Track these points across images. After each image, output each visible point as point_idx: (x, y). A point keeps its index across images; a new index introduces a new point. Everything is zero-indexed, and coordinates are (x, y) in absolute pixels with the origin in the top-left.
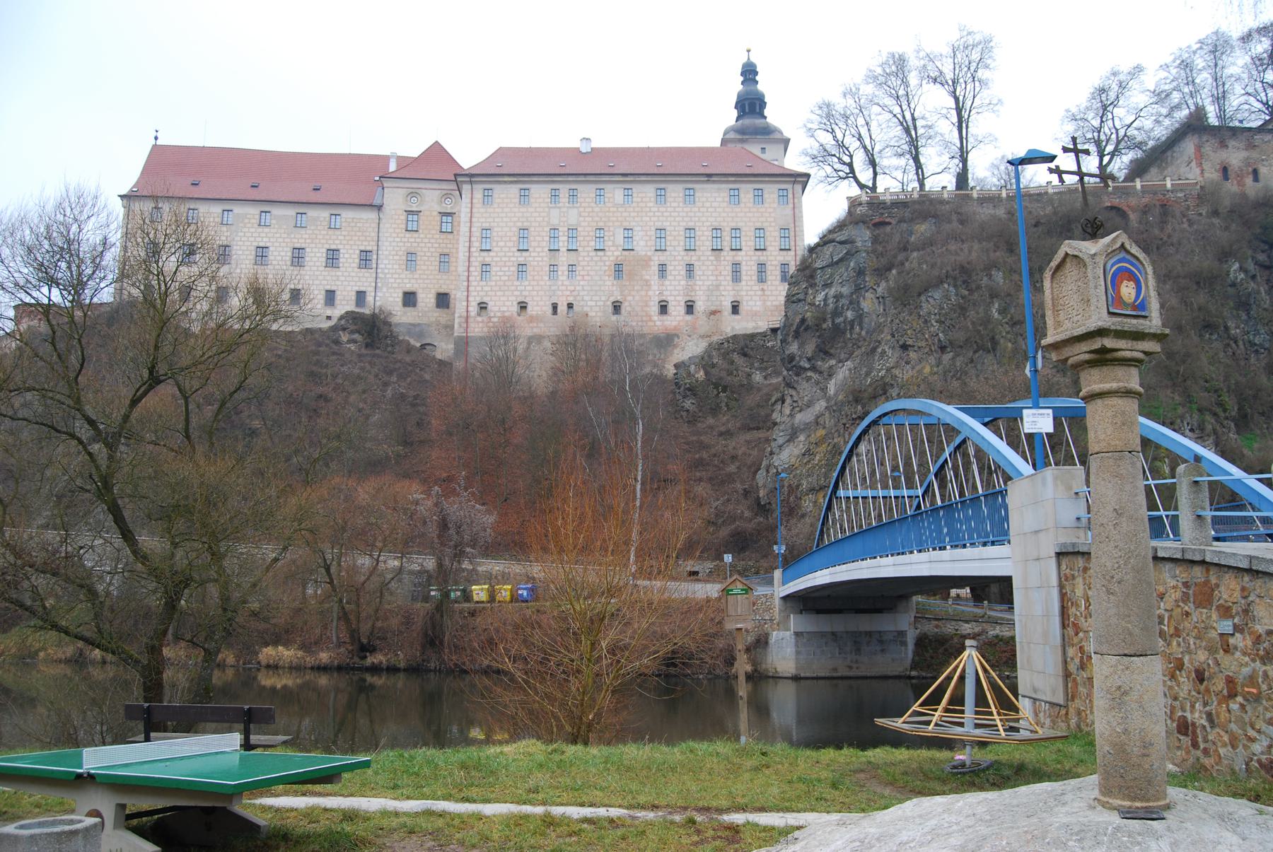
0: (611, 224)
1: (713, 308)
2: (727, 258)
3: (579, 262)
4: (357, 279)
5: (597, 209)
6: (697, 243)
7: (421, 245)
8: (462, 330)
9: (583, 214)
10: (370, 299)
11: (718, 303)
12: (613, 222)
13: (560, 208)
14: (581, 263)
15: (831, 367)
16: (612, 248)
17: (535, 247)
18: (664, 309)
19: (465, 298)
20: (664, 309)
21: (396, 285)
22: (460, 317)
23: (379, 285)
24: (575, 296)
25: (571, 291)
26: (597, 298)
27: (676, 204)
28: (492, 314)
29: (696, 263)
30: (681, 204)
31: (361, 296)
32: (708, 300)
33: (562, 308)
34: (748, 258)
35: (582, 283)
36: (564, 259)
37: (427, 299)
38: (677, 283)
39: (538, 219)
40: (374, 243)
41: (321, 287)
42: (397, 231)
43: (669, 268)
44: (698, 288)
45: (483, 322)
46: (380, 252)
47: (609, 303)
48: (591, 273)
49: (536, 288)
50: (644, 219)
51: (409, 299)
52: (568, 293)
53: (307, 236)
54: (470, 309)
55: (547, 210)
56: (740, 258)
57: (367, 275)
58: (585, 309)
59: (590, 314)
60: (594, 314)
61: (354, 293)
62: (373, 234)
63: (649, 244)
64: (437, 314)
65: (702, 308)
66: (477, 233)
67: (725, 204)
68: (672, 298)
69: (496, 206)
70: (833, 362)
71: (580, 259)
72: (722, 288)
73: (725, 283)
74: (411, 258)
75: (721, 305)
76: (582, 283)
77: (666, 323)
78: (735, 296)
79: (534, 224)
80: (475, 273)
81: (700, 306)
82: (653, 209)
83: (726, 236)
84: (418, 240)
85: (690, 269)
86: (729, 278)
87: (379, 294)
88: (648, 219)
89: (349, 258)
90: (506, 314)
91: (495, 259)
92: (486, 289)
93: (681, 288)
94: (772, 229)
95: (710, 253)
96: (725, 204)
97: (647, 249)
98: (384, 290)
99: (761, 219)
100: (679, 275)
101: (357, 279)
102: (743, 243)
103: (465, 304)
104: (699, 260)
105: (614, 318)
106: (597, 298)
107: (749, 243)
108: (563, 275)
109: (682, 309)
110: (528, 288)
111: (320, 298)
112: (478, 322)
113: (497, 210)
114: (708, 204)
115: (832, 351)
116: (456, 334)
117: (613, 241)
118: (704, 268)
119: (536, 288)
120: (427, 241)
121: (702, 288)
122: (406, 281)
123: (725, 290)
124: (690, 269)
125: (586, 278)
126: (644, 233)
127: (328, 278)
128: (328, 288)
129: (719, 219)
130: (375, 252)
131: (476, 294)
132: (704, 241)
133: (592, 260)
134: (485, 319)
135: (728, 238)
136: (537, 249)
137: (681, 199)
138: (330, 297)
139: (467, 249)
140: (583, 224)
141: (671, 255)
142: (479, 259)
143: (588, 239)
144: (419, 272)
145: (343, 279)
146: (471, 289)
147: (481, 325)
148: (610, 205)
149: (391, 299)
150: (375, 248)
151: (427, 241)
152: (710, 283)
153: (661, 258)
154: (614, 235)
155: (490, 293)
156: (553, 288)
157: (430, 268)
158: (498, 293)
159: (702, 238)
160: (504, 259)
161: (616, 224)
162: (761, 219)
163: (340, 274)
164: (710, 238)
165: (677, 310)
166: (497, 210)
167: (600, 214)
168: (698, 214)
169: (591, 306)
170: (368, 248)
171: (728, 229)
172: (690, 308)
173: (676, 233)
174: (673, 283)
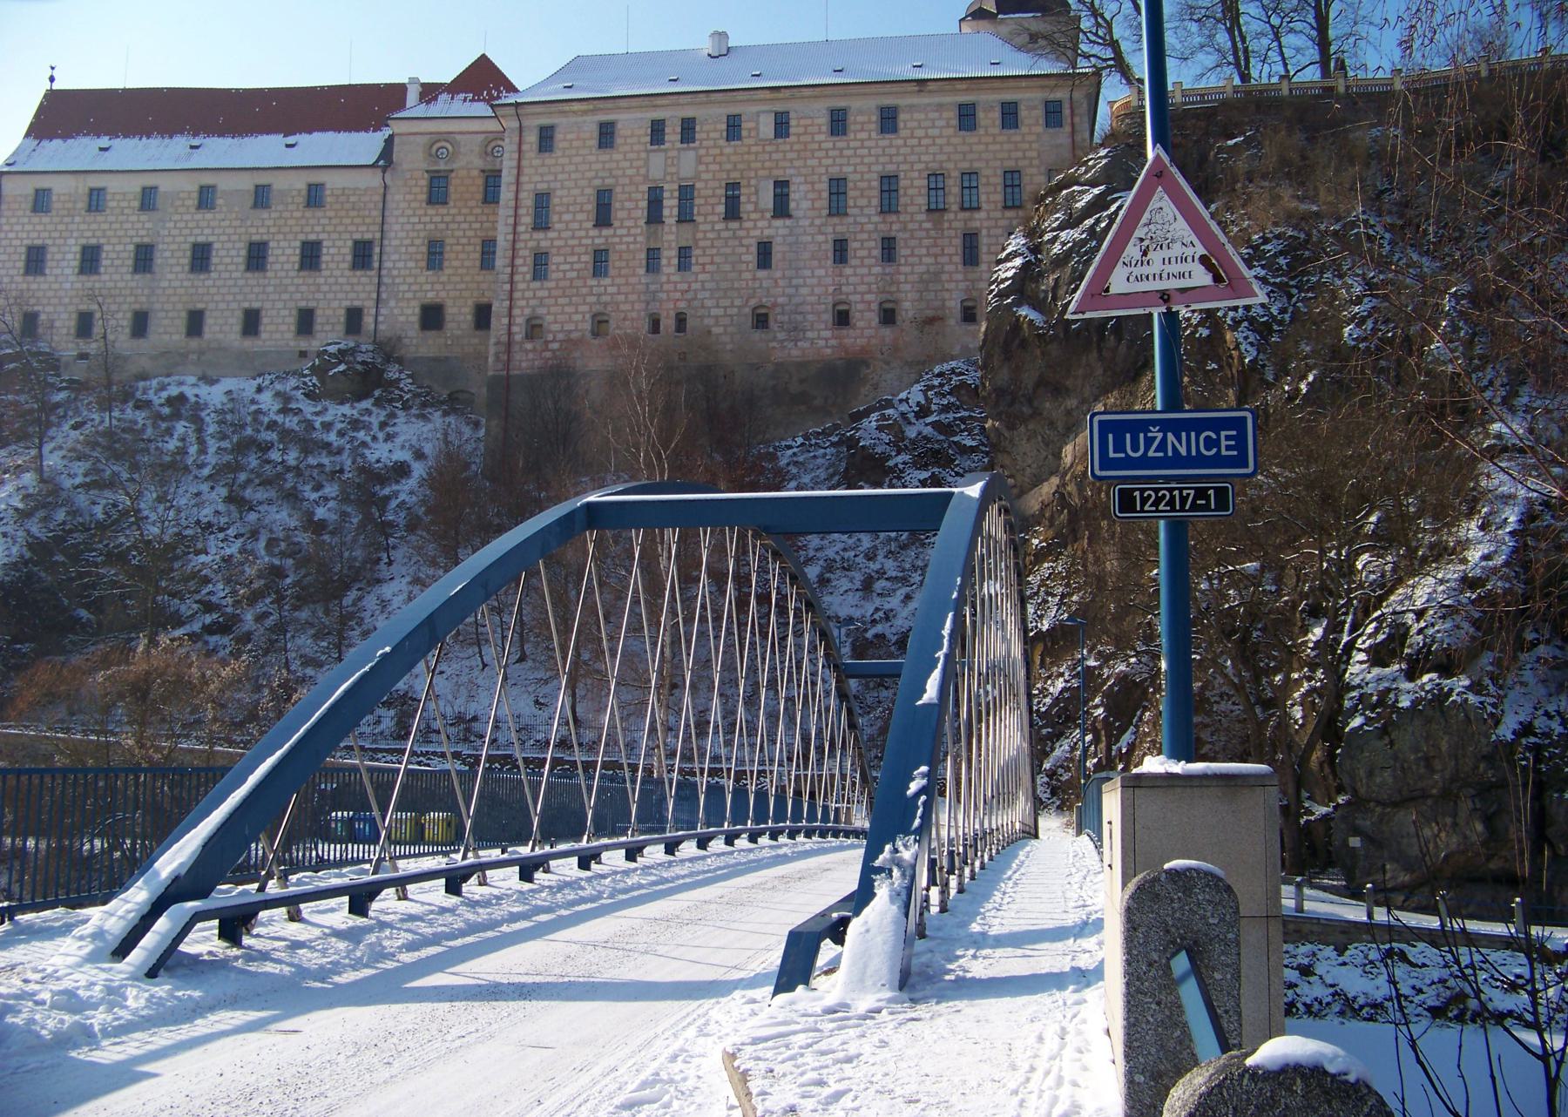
0: (752, 174)
1: (930, 313)
2: (956, 224)
3: (696, 241)
4: (348, 288)
5: (728, 150)
6: (902, 200)
7: (452, 226)
8: (500, 366)
9: (705, 160)
10: (368, 320)
11: (937, 304)
12: (756, 170)
13: (665, 151)
14: (701, 244)
15: (1069, 412)
16: (753, 216)
17: (622, 220)
18: (842, 319)
19: (506, 311)
20: (842, 319)
21: (409, 295)
22: (498, 343)
23: (384, 296)
24: (689, 301)
25: (684, 292)
26: (727, 302)
27: (864, 135)
28: (550, 337)
29: (900, 235)
30: (874, 135)
31: (354, 318)
32: (921, 299)
33: (668, 323)
34: (992, 223)
35: (701, 277)
36: (672, 237)
37: (459, 315)
38: (865, 271)
39: (629, 172)
40: (377, 228)
41: (292, 304)
42: (414, 205)
43: (853, 245)
44: (902, 278)
45: (534, 350)
46: (386, 242)
47: (747, 310)
48: (717, 259)
49: (623, 289)
50: (809, 162)
51: (432, 316)
52: (678, 295)
53: (271, 223)
54: (515, 329)
55: (643, 155)
56: (978, 224)
57: (364, 280)
58: (706, 321)
59: (716, 330)
60: (721, 330)
61: (343, 312)
62: (375, 213)
63: (817, 205)
64: (476, 341)
65: (911, 314)
66: (528, 201)
67: (951, 131)
68: (857, 297)
69: (559, 153)
70: (1072, 403)
71: (700, 235)
72: (945, 277)
73: (951, 268)
74: (435, 255)
75: (943, 307)
76: (701, 277)
77: (847, 341)
78: (967, 290)
79: (621, 181)
80: (525, 268)
81: (908, 308)
82: (824, 145)
83: (954, 189)
84: (447, 219)
85: (889, 249)
86: (958, 259)
87: (383, 311)
88: (815, 162)
89: (337, 253)
90: (574, 336)
91: (557, 243)
92: (540, 294)
93: (872, 279)
94: (1034, 171)
95: (923, 217)
96: (951, 131)
97: (816, 213)
98: (392, 303)
99: (1014, 155)
100: (870, 256)
101: (348, 288)
102: (983, 198)
103: (505, 321)
104: (905, 229)
105: (757, 335)
106: (727, 302)
107: (994, 197)
108: (669, 265)
109: (874, 318)
110: (610, 290)
111: (125, 321)
112: (527, 352)
113: (561, 161)
114: (920, 133)
115: (1069, 383)
116: (490, 373)
117: (756, 204)
118: (913, 243)
119: (623, 289)
120: (461, 218)
121: (910, 278)
122: (428, 287)
123: (951, 281)
124: (889, 249)
125: (708, 267)
126: (809, 187)
127: (304, 288)
128: (303, 304)
129: (939, 157)
130: (377, 243)
131: (523, 303)
132: (913, 192)
133: (719, 238)
134: (539, 344)
135: (956, 190)
136: (627, 223)
137: (873, 126)
138: (305, 321)
139: (510, 229)
140: (704, 176)
141: (856, 223)
142: (531, 244)
143: (712, 201)
144: (448, 271)
145: (325, 288)
146: (517, 295)
147: (531, 356)
148: (751, 141)
149: (402, 319)
150: (378, 235)
151: (461, 218)
152: (923, 269)
153: (839, 229)
154: (757, 193)
155: (547, 301)
156: (653, 287)
157: (467, 263)
158: (561, 301)
159: (910, 192)
160: (571, 242)
161: (761, 173)
162: (1014, 155)
163: (322, 280)
164: (924, 191)
165: (866, 320)
166: (561, 161)
167: (733, 158)
168: (902, 151)
169: (717, 317)
170: (368, 236)
171: (956, 174)
172: (888, 316)
173: (865, 185)
174: (859, 271)
